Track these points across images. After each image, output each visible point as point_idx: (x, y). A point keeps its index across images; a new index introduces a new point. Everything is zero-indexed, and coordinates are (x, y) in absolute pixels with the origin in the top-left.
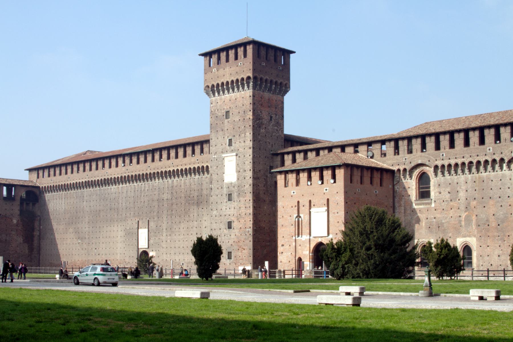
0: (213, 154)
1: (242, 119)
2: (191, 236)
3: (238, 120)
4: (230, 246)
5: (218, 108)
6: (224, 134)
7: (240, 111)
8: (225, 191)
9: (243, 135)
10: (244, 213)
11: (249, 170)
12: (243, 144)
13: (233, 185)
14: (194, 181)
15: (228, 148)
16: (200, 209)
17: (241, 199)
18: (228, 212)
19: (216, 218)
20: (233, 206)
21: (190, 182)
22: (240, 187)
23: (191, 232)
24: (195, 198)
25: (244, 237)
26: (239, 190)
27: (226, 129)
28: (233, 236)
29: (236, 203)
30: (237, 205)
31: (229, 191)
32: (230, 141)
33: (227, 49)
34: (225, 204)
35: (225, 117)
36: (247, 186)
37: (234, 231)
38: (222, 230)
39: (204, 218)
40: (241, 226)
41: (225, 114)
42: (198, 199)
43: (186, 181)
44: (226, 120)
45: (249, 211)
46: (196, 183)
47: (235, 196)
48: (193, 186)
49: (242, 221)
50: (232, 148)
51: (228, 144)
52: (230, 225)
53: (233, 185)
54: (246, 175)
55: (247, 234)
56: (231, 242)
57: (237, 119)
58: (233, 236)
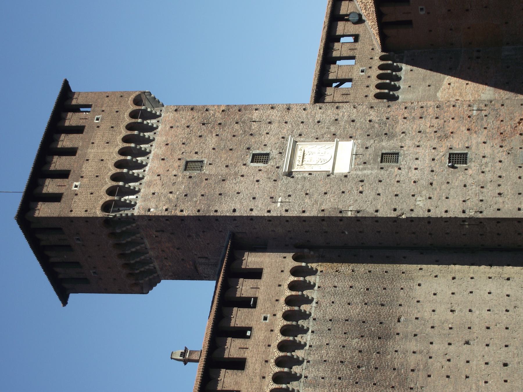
0: (272, 207)
1: (217, 128)
2: (473, 363)
3: (215, 139)
4: (511, 157)
5: (166, 191)
6: (236, 174)
7: (199, 134)
8: (372, 172)
9: (255, 126)
10: (435, 121)
11: (336, 111)
12: (274, 126)
13: (361, 151)
14: (320, 346)
15: (271, 163)
16: (400, 328)
17: (399, 129)
18: (425, 163)
19: (435, 198)
20: (412, 150)
21: (316, 363)
22: (371, 132)
23: (463, 363)
24: (364, 345)
25: (490, 119)
26: (377, 135)
27: (225, 171)
28: (487, 150)
29: (408, 142)
30: (412, 138)
31: (375, 160)
32: (255, 158)
33: (48, 149)
34: (403, 172)
35: (195, 173)
36: (373, 115)
37: (474, 148)
38: (470, 181)
39: (427, 315)
40: (464, 129)
41: (188, 173)
42: (371, 335)
43: (310, 376)
44: (206, 170)
45: (431, 110)
46: (325, 341)
47: (387, 146)
48: (332, 353)
49: (451, 125)
50: (274, 153)
51: (261, 165)
52: (457, 159)
53: (361, 151)
54: (346, 118)
55: (484, 113)
56: (501, 154)
57: (212, 141)
58: (487, 150)
